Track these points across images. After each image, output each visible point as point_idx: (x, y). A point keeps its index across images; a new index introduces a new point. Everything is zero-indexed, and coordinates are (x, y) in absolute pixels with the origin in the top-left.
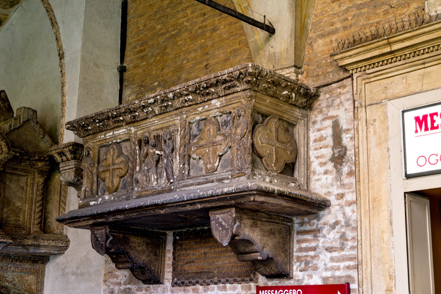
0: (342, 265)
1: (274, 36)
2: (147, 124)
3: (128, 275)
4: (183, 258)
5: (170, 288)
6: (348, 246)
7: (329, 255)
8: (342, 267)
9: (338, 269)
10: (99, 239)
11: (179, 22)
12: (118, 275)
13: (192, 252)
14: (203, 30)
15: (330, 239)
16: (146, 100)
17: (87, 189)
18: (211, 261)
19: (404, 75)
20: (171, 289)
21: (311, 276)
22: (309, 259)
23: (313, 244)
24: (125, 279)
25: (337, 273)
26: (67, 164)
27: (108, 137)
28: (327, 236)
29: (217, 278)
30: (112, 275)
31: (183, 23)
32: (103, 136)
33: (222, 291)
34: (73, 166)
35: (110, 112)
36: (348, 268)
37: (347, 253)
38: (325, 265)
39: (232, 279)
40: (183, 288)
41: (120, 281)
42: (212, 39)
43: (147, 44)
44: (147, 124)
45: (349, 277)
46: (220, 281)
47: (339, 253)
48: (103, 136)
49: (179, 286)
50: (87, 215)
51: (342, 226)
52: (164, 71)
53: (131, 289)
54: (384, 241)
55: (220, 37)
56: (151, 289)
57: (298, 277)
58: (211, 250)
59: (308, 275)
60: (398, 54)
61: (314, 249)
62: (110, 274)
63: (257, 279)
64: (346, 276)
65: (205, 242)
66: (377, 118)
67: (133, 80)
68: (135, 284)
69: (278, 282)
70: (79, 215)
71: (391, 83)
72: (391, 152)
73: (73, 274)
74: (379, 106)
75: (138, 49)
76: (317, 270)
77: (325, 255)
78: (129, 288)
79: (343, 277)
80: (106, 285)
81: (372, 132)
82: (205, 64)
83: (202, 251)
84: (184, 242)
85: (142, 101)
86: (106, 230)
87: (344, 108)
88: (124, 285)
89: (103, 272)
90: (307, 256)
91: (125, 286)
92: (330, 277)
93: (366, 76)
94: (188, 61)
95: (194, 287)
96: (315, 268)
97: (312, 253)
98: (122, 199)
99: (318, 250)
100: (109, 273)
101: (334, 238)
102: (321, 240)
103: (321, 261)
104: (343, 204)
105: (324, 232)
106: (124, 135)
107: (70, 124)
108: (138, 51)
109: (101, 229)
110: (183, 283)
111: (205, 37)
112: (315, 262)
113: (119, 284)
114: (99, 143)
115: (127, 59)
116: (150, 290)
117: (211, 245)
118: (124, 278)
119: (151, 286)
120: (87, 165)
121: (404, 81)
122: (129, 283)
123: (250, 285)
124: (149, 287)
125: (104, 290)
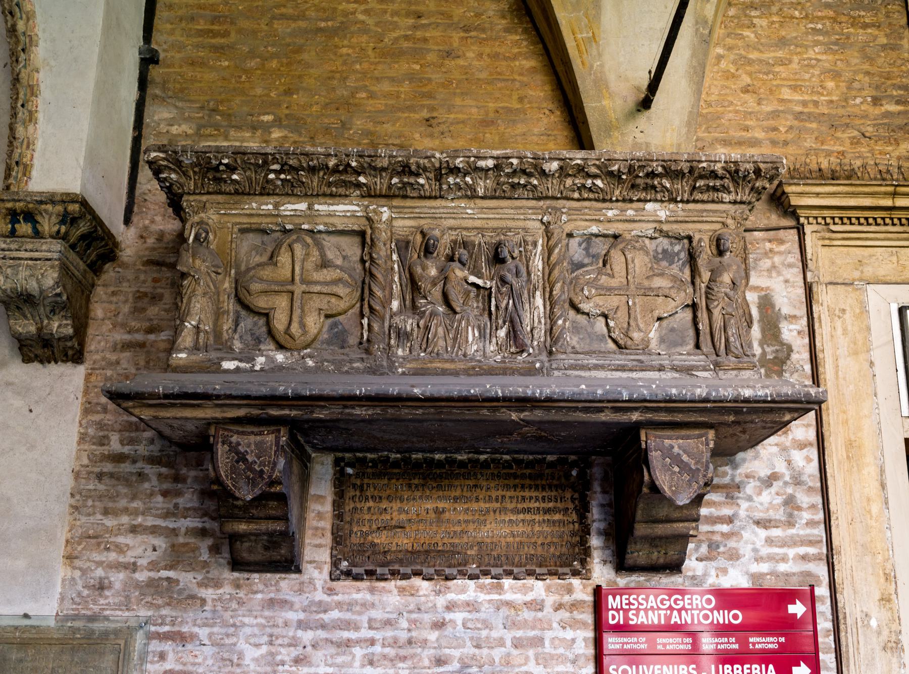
0: (792, 552)
1: (647, 113)
2: (437, 211)
3: (164, 546)
4: (367, 517)
5: (322, 582)
6: (801, 519)
7: (762, 533)
8: (791, 556)
9: (784, 559)
10: (250, 458)
11: (340, 7)
12: (127, 545)
13: (396, 505)
14: (417, 46)
15: (761, 504)
16: (472, 159)
17: (201, 326)
18: (458, 529)
19: (894, 250)
20: (328, 586)
21: (725, 571)
22: (717, 538)
23: (726, 511)
24: (154, 556)
25: (782, 567)
26: (29, 246)
27: (288, 213)
28: (755, 498)
29: (477, 567)
30: (99, 544)
31: (353, 13)
32: (270, 207)
33: (489, 593)
34: (56, 256)
35: (336, 156)
36: (804, 558)
37: (802, 532)
38: (755, 550)
39: (523, 569)
40: (368, 583)
41: (132, 560)
42: (444, 70)
43: (232, 23)
44: (437, 211)
45: (809, 574)
46: (486, 573)
47: (784, 530)
48: (270, 207)
49: (357, 578)
50: (254, 394)
51: (786, 483)
52: (295, 96)
53: (177, 581)
54: (871, 516)
55: (467, 73)
56: (255, 583)
57: (694, 570)
58: (456, 505)
59: (717, 569)
60: (896, 214)
61: (730, 520)
62: (93, 541)
63: (589, 571)
64: (802, 573)
65: (439, 487)
66: (848, 308)
67: (182, 90)
68: (194, 569)
69: (642, 578)
70: (215, 389)
71: (871, 256)
72: (877, 369)
74: (849, 289)
75: (201, 25)
76: (738, 559)
77: (756, 535)
79: (794, 574)
80: (74, 568)
81: (839, 331)
82: (425, 114)
83: (430, 505)
84: (371, 482)
85: (459, 157)
86: (277, 439)
87: (781, 278)
88: (150, 570)
89: (62, 535)
90: (713, 532)
91: (152, 574)
92: (767, 574)
93: (828, 235)
94: (372, 96)
95: (404, 583)
96: (734, 556)
97: (725, 528)
98: (353, 368)
99: (737, 523)
100: (90, 537)
101: (771, 503)
102: (744, 505)
103: (746, 543)
104: (788, 444)
105: (750, 489)
106: (346, 220)
107: (165, 152)
108: (201, 30)
109: (261, 434)
110: (370, 574)
111: (422, 62)
112: (732, 544)
113: (133, 567)
114: (246, 220)
115: (156, 36)
116: (251, 585)
117: (458, 493)
118: (149, 552)
119: (256, 575)
120: (207, 267)
121: (894, 259)
122: (171, 567)
123: (571, 584)
124: (248, 579)
125: (63, 580)
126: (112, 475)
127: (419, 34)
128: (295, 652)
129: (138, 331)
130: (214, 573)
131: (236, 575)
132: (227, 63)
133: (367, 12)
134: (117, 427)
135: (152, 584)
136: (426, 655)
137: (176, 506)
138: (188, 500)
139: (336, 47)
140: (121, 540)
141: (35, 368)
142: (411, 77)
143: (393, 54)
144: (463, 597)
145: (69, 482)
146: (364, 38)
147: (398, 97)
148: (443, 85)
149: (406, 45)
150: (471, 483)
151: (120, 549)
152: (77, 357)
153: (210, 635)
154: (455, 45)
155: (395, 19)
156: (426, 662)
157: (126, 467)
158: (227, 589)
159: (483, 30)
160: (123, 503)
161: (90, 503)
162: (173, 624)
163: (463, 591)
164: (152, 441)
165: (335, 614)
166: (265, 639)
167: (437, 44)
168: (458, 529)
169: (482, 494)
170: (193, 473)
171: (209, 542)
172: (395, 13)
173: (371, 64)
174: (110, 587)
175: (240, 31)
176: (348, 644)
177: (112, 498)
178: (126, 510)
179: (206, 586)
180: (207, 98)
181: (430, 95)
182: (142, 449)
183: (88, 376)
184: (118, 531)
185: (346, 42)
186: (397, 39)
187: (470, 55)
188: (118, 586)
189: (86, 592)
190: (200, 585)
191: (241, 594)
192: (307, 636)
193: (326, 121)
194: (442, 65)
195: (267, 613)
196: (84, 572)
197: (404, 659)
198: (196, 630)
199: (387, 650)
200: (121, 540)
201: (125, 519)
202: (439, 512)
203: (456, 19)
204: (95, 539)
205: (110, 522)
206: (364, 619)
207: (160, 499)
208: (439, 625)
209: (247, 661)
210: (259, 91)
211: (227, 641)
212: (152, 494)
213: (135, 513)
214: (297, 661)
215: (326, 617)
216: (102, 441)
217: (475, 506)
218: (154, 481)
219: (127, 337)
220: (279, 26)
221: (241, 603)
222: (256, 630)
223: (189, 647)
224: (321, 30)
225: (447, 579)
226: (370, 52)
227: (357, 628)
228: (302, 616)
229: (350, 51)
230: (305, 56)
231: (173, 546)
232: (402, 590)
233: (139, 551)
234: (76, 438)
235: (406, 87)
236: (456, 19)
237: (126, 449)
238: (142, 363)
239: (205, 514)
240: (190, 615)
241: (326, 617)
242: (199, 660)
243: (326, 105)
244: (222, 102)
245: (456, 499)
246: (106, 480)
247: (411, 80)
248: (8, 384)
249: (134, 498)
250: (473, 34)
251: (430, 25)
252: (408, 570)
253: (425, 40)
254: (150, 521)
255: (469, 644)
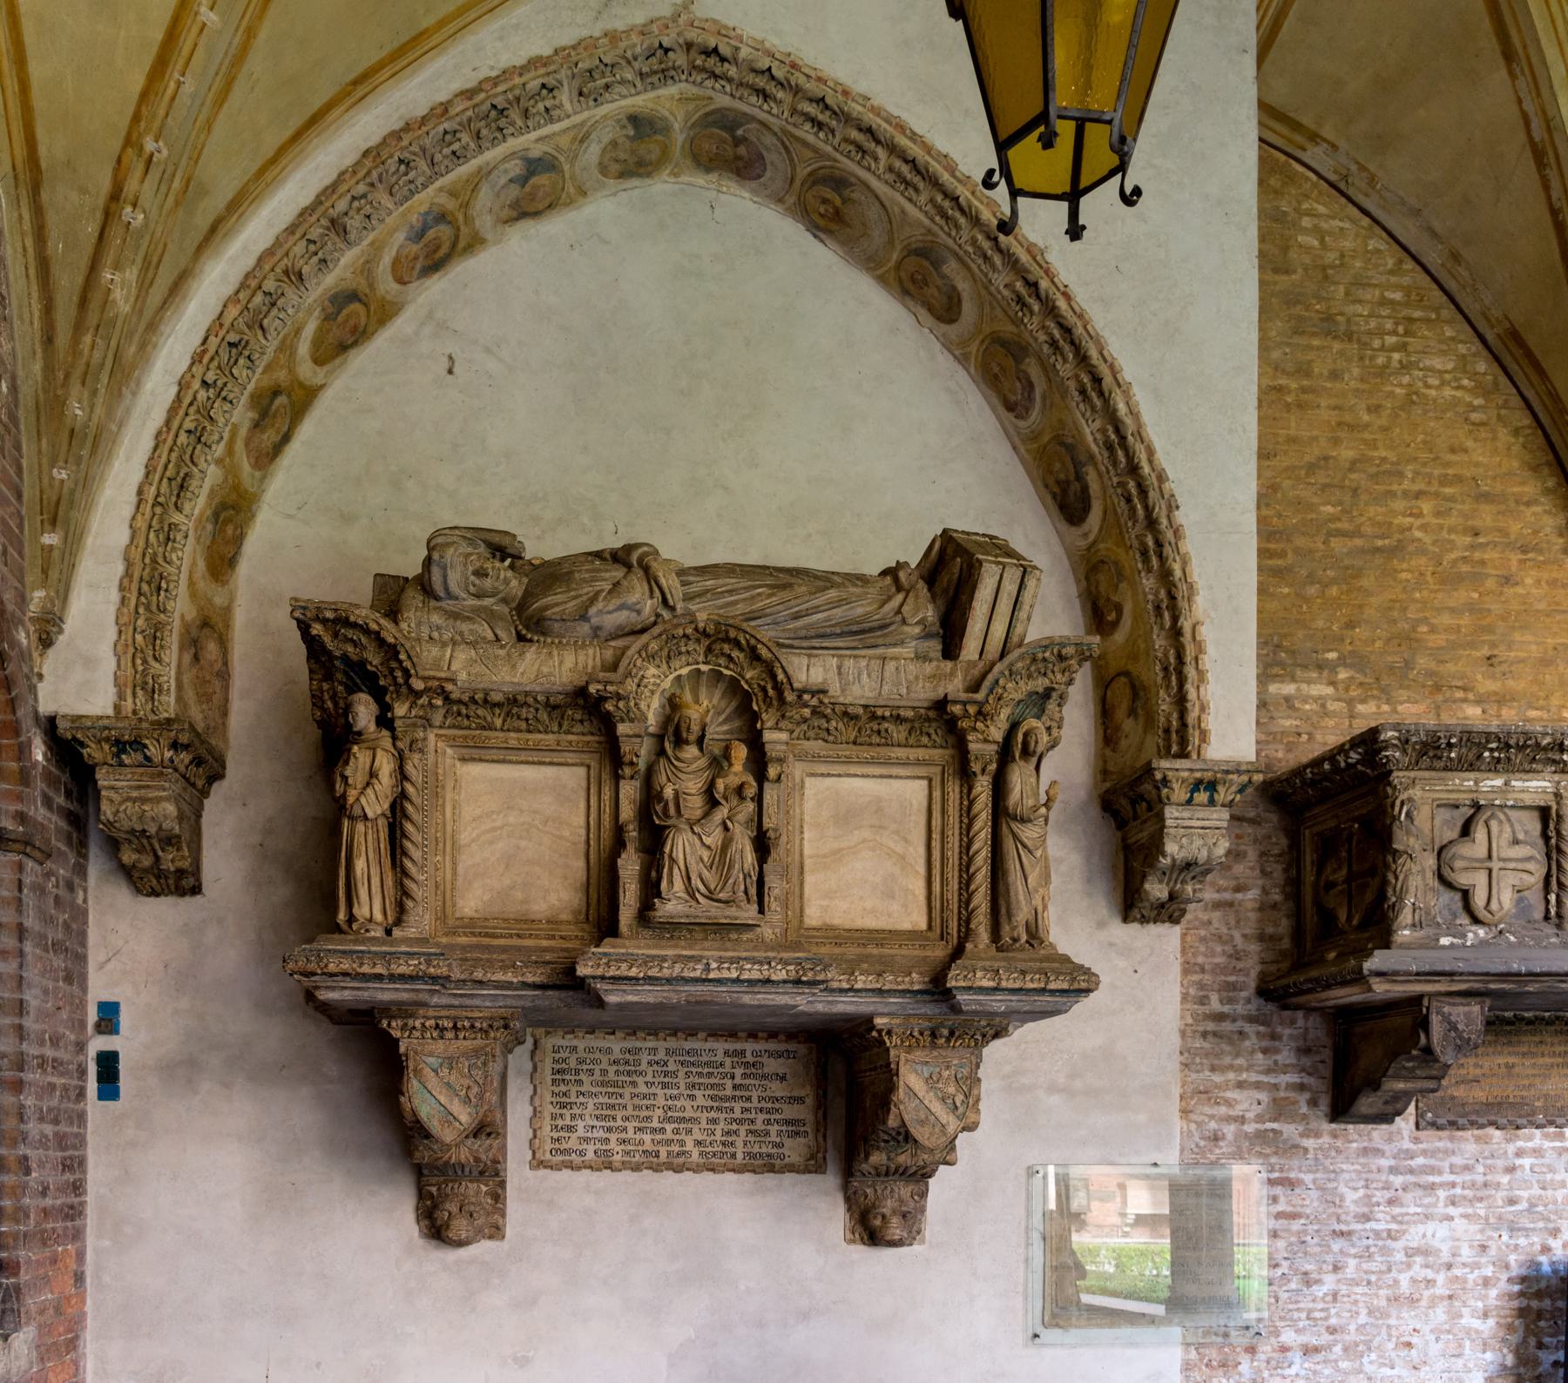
11: (1396, 522)
13: (1472, 1061)
18: (1526, 1082)
24: (1259, 1109)
31: (1410, 529)
43: (1289, 540)
46: (1551, 1123)
53: (1281, 1133)
65: (1510, 1043)
73: (1053, 1089)
78: (1273, 1130)
82: (1486, 651)
83: (1501, 1060)
89: (1176, 1091)
94: (1433, 630)
95: (1477, 1132)
110: (1453, 1125)
113: (1242, 1120)
117: (1525, 1049)
118: (1255, 1106)
119: (1350, 1127)
122: (1275, 1120)
126: (1215, 1034)
127: (1477, 555)
128: (1388, 1195)
129: (1225, 890)
130: (1314, 1125)
131: (1333, 1126)
132: (1286, 590)
133: (1424, 528)
134: (1216, 987)
135: (1260, 1136)
136: (1500, 1196)
137: (1276, 1062)
138: (1286, 1056)
139: (1395, 571)
140: (1229, 1094)
141: (1134, 927)
142: (1472, 608)
143: (1452, 580)
144: (1530, 1144)
145: (1176, 1040)
146: (1423, 561)
147: (1459, 631)
148: (1503, 619)
149: (1465, 568)
150: (1537, 1039)
151: (1229, 1103)
152: (1174, 920)
153: (1314, 1181)
154: (1514, 569)
155: (1453, 537)
156: (1500, 1203)
157: (1227, 1026)
158: (1326, 1140)
159: (1541, 552)
160: (1227, 1060)
161: (1198, 1060)
162: (1281, 1170)
163: (1530, 1139)
164: (1249, 1001)
165: (1420, 1161)
166: (1362, 1183)
167: (1496, 568)
168: (1526, 1082)
169: (1546, 1049)
170: (1287, 1031)
171: (1307, 1095)
172: (1451, 530)
173: (1432, 591)
174: (1223, 1138)
175: (1297, 551)
176: (1432, 1187)
177: (1217, 1056)
178: (1231, 1067)
179: (1308, 1137)
180: (1270, 631)
181: (1490, 629)
182: (1240, 1008)
183: (1184, 936)
184: (1225, 1086)
185: (1405, 566)
186: (1455, 561)
187: (1529, 581)
188: (1230, 1137)
189: (1202, 1143)
190: (1302, 1135)
191: (1339, 1144)
192: (1398, 1180)
193: (1390, 659)
194: (1501, 593)
195: (1362, 1160)
196: (1199, 1124)
197: (1481, 1199)
198: (1302, 1176)
199: (1466, 1192)
200: (1229, 1094)
201: (1231, 1075)
202: (1510, 1067)
203: (1513, 537)
204: (1205, 1094)
205: (1217, 1078)
206: (1446, 1164)
207: (1260, 1055)
208: (1511, 1170)
209: (1348, 1203)
210: (1320, 623)
211: (1330, 1185)
212: (1253, 1052)
213: (1239, 1069)
214: (1390, 1202)
215: (1412, 1163)
216: (1203, 1001)
217: (1541, 1061)
218: (1254, 1039)
219: (1216, 896)
220: (1337, 544)
221: (1339, 1151)
222: (1354, 1175)
223: (1297, 1191)
224: (1378, 550)
225: (1518, 1128)
226: (1429, 578)
227: (1440, 1173)
228: (1392, 1162)
229: (1409, 576)
230: (1364, 582)
231: (1274, 1100)
232: (1478, 1139)
233: (1245, 1106)
234: (1178, 998)
235: (1466, 620)
236: (1513, 537)
237: (1226, 1009)
238: (1233, 923)
239: (1303, 1070)
240: (1295, 1163)
241: (1412, 1163)
242: (1307, 1202)
243: (1389, 640)
244: (1285, 636)
245: (1524, 1055)
246: (1210, 1038)
247: (1471, 611)
248: (1111, 944)
249: (1237, 1055)
250: (1531, 555)
251: (1488, 544)
252: (1481, 1121)
253: (1483, 563)
254: (1254, 1077)
255: (1536, 1186)
